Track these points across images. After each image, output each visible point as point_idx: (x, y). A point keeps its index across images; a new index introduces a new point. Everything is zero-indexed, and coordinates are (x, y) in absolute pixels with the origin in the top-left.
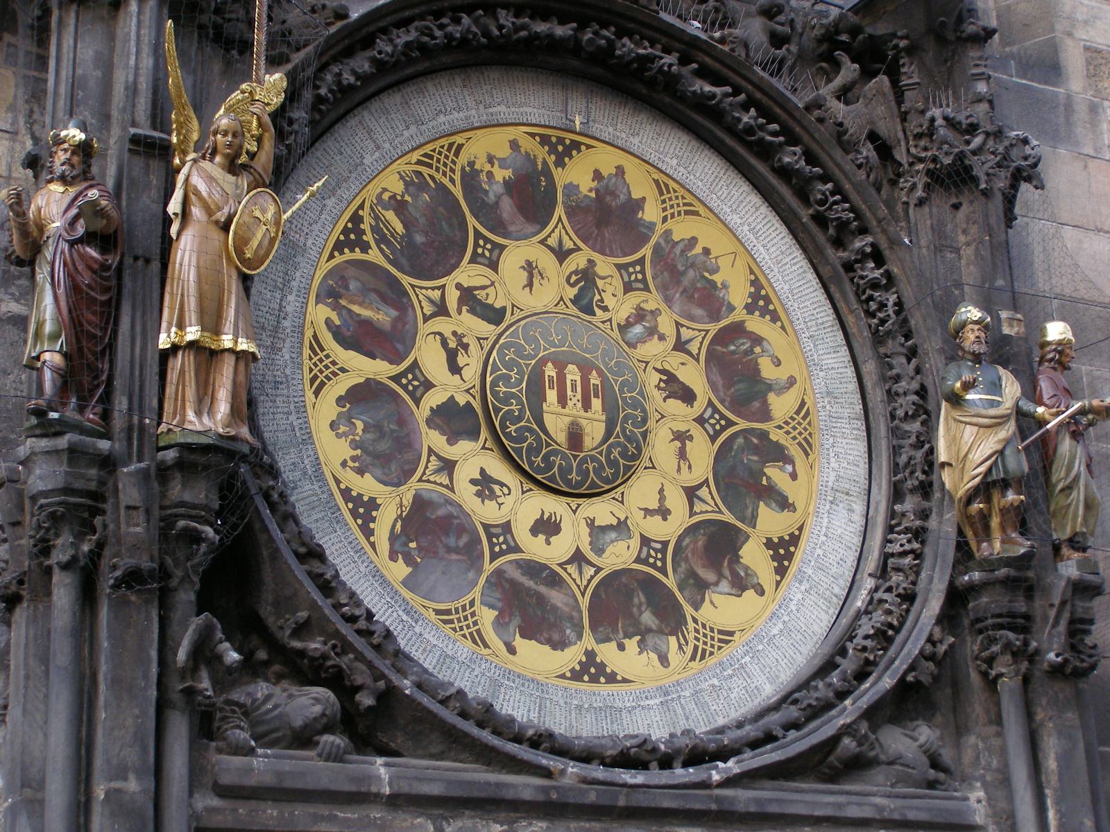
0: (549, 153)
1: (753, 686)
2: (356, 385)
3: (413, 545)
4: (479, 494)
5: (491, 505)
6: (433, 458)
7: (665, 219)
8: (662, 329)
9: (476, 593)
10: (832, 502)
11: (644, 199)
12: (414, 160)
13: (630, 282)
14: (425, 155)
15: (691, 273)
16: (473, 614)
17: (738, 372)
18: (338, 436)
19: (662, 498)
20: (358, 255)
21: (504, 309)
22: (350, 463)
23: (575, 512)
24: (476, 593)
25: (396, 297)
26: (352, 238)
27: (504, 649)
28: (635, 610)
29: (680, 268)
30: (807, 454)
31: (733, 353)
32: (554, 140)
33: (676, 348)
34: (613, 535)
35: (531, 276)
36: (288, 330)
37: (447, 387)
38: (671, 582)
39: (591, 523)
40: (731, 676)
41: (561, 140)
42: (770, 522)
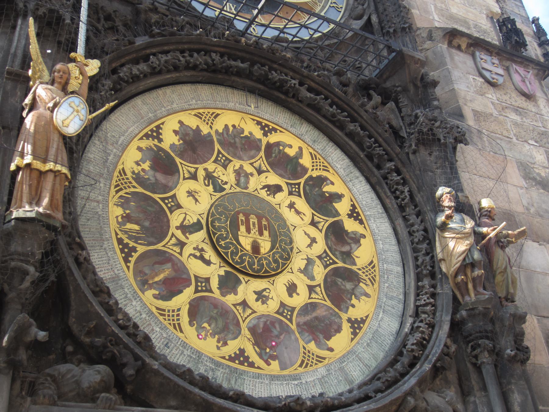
0: (153, 140)
1: (395, 273)
3: (268, 350)
5: (270, 302)
6: (238, 307)
7: (211, 127)
8: (249, 172)
9: (301, 343)
10: (350, 181)
11: (198, 126)
12: (114, 193)
13: (223, 164)
15: (237, 140)
16: (309, 352)
18: (205, 339)
19: (308, 235)
20: (135, 255)
21: (198, 220)
22: (220, 345)
23: (292, 273)
24: (301, 343)
25: (163, 258)
27: (328, 352)
28: (342, 287)
29: (232, 141)
31: (276, 157)
32: (150, 133)
33: (259, 174)
34: (310, 267)
36: (147, 318)
38: (340, 264)
40: (388, 278)
41: (152, 130)
42: (343, 207)
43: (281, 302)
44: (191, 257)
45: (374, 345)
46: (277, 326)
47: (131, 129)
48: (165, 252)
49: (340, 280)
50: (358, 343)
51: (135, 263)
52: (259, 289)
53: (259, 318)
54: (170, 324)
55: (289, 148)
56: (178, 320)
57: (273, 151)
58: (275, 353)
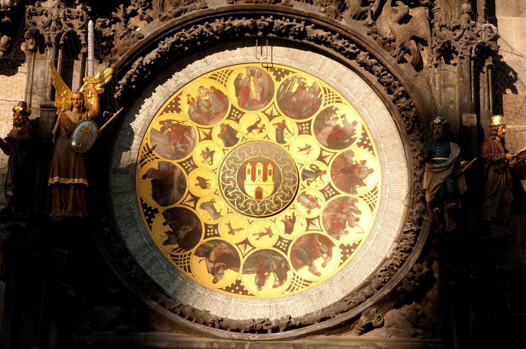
0: (361, 139)
2: (223, 93)
3: (170, 130)
4: (203, 152)
6: (209, 130)
7: (361, 197)
8: (312, 211)
10: (270, 306)
11: (365, 185)
13: (326, 191)
14: (329, 90)
17: (310, 249)
20: (274, 78)
22: (190, 98)
24: (162, 159)
25: (266, 97)
26: (280, 74)
27: (143, 174)
28: (184, 227)
29: (344, 211)
30: (288, 290)
31: (318, 245)
32: (367, 138)
34: (212, 212)
35: (305, 149)
37: (241, 128)
39: (213, 201)
40: (170, 273)
41: (369, 141)
42: (249, 281)
43: (197, 167)
44: (259, 119)
45: (127, 213)
46: (182, 150)
47: (373, 123)
48: (269, 101)
49: (190, 230)
50: (137, 201)
51: (268, 75)
52: (215, 156)
53: (194, 140)
54: (218, 73)
55: (323, 264)
56: (219, 81)
57: (324, 246)
58: (165, 133)
